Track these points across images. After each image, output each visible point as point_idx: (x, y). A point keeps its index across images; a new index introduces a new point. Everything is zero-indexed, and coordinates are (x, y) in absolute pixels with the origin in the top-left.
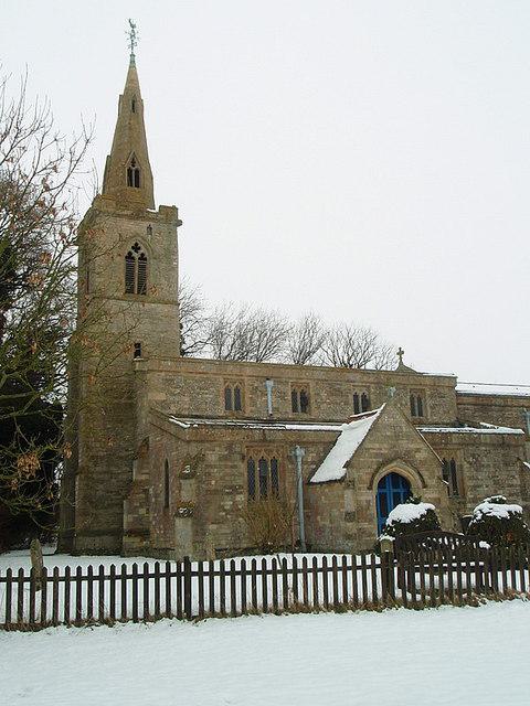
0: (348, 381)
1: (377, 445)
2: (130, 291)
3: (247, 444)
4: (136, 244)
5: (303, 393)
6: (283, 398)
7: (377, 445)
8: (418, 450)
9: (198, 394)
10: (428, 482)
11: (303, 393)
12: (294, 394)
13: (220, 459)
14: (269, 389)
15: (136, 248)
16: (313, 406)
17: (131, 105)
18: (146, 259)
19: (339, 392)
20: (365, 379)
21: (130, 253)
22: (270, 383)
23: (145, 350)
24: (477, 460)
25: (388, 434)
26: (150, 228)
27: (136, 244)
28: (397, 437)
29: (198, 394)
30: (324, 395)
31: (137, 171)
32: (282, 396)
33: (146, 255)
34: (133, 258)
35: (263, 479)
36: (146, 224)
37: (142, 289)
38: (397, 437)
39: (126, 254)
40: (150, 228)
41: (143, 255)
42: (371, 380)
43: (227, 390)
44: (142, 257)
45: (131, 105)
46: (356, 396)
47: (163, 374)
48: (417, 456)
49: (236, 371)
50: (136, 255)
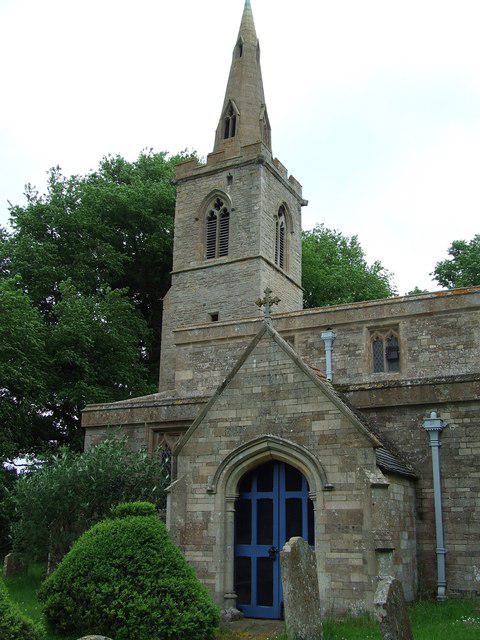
1: (232, 414)
6: (352, 354)
7: (232, 414)
8: (319, 416)
10: (336, 477)
11: (393, 339)
12: (376, 342)
14: (328, 345)
15: (218, 205)
16: (405, 358)
17: (246, 52)
19: (455, 328)
22: (326, 335)
25: (257, 390)
27: (218, 200)
28: (274, 394)
30: (424, 338)
31: (234, 120)
32: (351, 351)
36: (225, 174)
39: (208, 214)
40: (230, 178)
41: (225, 210)
45: (246, 52)
47: (191, 347)
48: (317, 427)
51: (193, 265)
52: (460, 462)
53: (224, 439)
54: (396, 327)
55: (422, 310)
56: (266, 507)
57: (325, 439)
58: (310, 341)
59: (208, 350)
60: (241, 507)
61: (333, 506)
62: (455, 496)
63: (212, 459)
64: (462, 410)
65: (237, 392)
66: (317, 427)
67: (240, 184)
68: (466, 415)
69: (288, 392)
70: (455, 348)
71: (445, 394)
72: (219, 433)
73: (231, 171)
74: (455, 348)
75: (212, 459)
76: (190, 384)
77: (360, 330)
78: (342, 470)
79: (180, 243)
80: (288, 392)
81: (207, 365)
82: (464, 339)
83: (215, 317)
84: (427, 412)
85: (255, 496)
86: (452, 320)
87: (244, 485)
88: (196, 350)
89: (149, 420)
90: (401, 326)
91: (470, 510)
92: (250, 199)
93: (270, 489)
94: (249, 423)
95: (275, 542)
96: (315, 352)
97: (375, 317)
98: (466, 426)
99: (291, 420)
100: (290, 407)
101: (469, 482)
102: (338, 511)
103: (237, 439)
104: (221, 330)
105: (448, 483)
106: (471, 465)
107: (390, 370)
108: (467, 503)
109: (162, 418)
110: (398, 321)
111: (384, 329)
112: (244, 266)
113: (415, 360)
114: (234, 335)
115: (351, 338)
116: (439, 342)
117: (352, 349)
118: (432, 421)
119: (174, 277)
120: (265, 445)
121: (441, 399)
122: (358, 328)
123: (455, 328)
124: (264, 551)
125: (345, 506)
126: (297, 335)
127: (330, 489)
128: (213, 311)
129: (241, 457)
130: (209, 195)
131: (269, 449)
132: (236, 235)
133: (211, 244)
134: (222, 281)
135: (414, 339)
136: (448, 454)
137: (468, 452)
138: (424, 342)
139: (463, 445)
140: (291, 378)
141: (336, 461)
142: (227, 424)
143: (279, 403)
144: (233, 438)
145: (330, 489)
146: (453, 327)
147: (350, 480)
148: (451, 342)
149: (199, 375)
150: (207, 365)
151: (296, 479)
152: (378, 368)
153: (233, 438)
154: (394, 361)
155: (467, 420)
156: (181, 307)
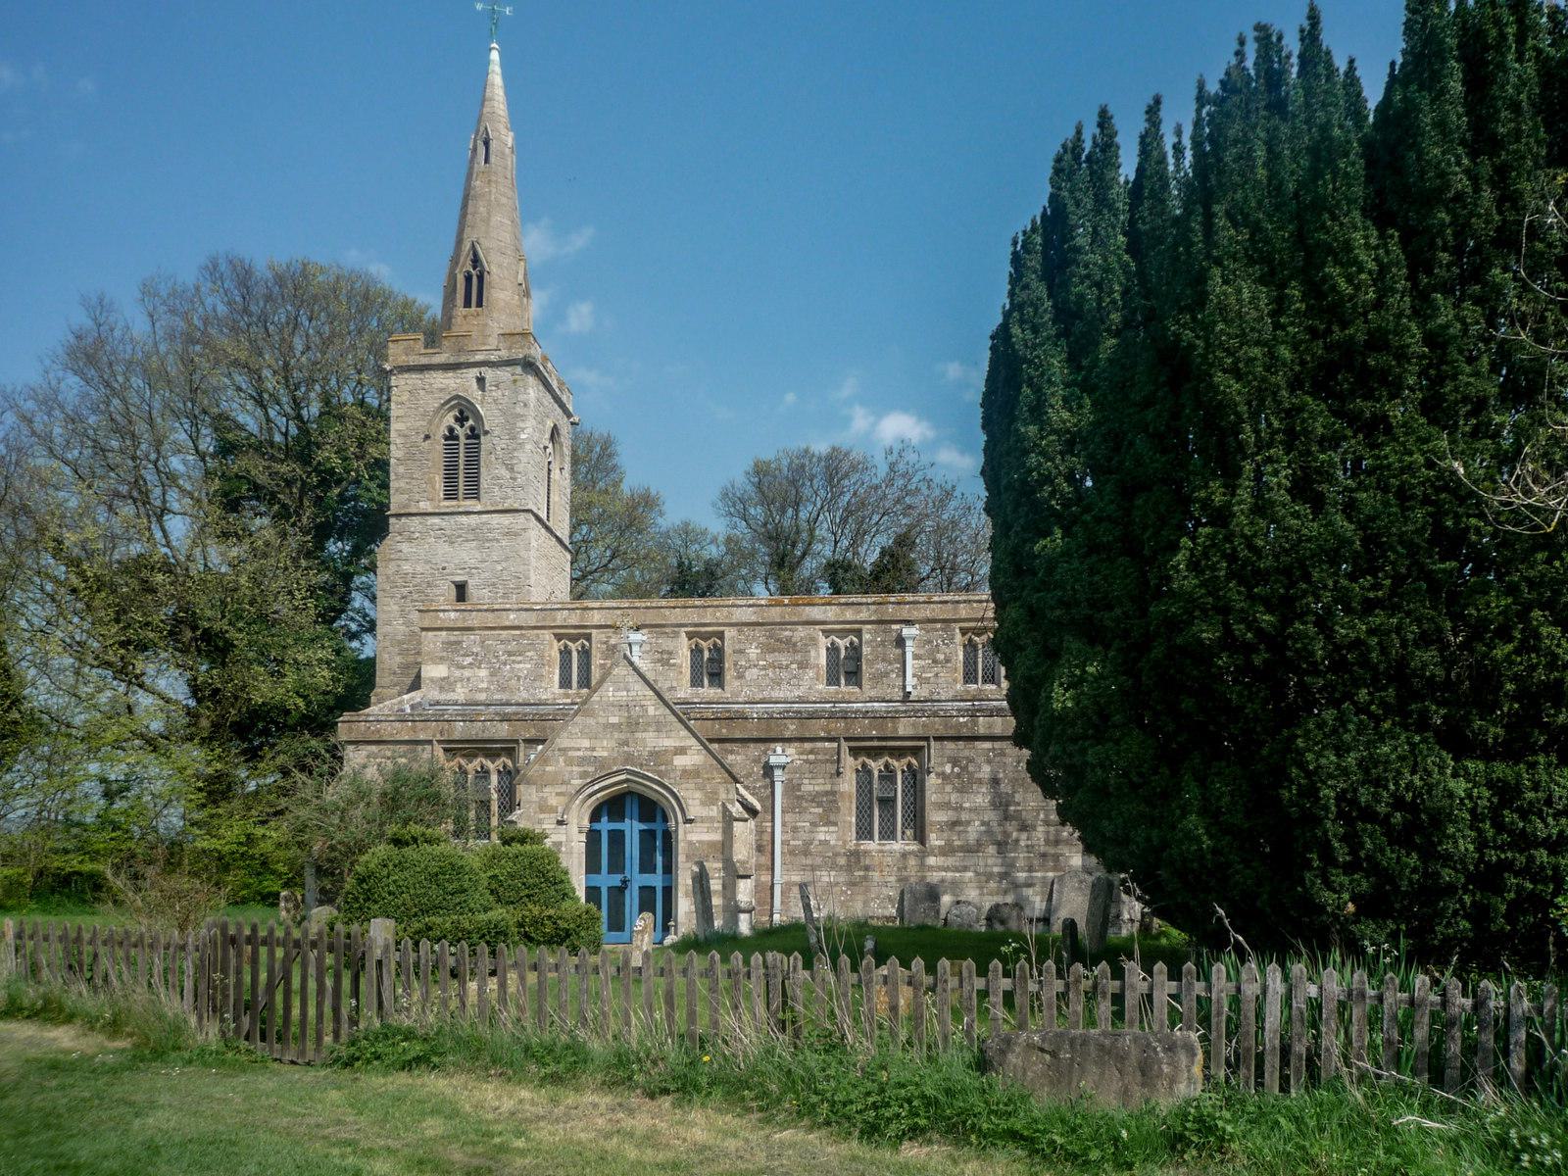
1: (586, 743)
2: (451, 494)
6: (665, 663)
7: (586, 743)
8: (682, 751)
11: (718, 652)
12: (696, 652)
16: (729, 675)
19: (790, 645)
20: (849, 615)
23: (472, 591)
24: (964, 769)
25: (614, 720)
28: (633, 725)
29: (505, 664)
30: (753, 652)
37: (474, 493)
38: (633, 725)
42: (864, 615)
43: (565, 653)
46: (833, 650)
47: (444, 633)
48: (680, 761)
51: (424, 506)
52: (801, 798)
53: (575, 768)
54: (721, 635)
55: (753, 619)
56: (617, 838)
57: (688, 774)
58: (613, 641)
59: (470, 640)
60: (593, 838)
61: (694, 837)
62: (795, 829)
63: (563, 789)
64: (808, 746)
65: (591, 721)
66: (680, 761)
67: (497, 394)
68: (811, 752)
69: (648, 724)
70: (787, 666)
71: (792, 729)
72: (570, 762)
73: (489, 374)
74: (787, 666)
75: (563, 789)
76: (445, 684)
77: (676, 635)
78: (703, 804)
79: (401, 469)
80: (648, 724)
81: (469, 660)
82: (798, 657)
83: (461, 591)
84: (772, 746)
85: (605, 826)
86: (787, 633)
87: (595, 817)
88: (452, 638)
89: (439, 737)
90: (726, 634)
91: (808, 843)
92: (512, 421)
93: (622, 819)
94: (605, 754)
95: (627, 874)
97: (696, 620)
98: (807, 761)
99: (651, 754)
100: (652, 741)
101: (808, 817)
102: (699, 842)
103: (591, 769)
104: (490, 615)
105: (789, 817)
106: (813, 801)
107: (711, 684)
108: (805, 836)
109: (456, 736)
110: (721, 629)
111: (706, 637)
112: (505, 520)
113: (741, 676)
114: (507, 624)
115: (666, 643)
116: (770, 658)
118: (780, 755)
119: (392, 520)
120: (623, 777)
121: (787, 735)
122: (674, 632)
123: (790, 645)
124: (616, 880)
125: (706, 837)
126: (594, 632)
127: (691, 821)
128: (458, 579)
129: (596, 787)
130: (443, 405)
131: (627, 781)
132: (491, 473)
133: (450, 478)
135: (741, 652)
136: (792, 788)
137: (811, 788)
138: (753, 656)
139: (806, 781)
140: (651, 711)
141: (698, 795)
142: (580, 753)
143: (639, 735)
144: (586, 768)
145: (691, 821)
146: (789, 641)
147: (711, 814)
148: (784, 659)
149: (458, 673)
150: (469, 660)
151: (650, 809)
152: (696, 682)
153: (586, 768)
154: (717, 677)
155: (812, 757)
156: (406, 567)
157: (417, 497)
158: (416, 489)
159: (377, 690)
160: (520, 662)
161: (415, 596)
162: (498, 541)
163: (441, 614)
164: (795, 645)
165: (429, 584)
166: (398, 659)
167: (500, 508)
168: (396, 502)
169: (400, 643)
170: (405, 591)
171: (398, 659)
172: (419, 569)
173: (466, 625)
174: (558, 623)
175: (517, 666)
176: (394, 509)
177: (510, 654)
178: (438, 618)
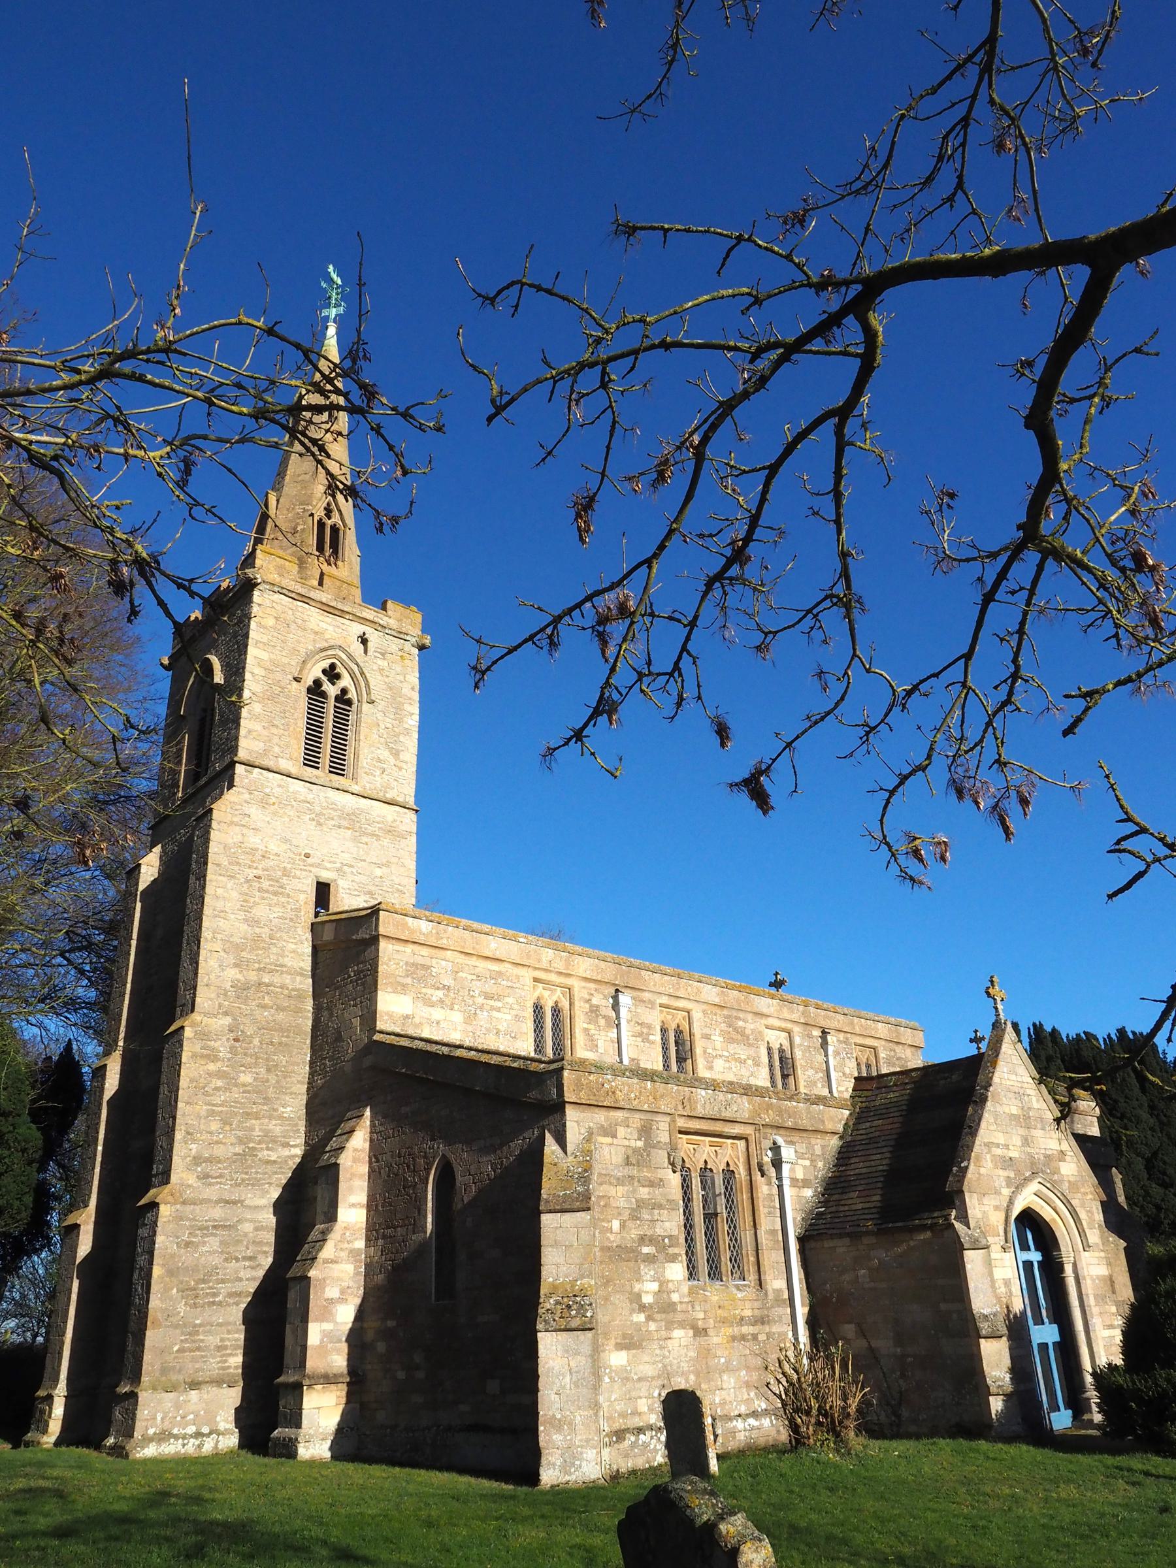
0: (758, 1014)
2: (311, 760)
3: (682, 1123)
4: (333, 666)
5: (678, 1032)
6: (646, 1040)
9: (482, 1008)
12: (664, 1031)
13: (628, 1162)
15: (332, 674)
18: (349, 703)
21: (317, 683)
26: (364, 641)
30: (718, 1039)
33: (352, 694)
34: (323, 695)
35: (710, 1217)
36: (357, 629)
39: (310, 682)
41: (344, 691)
44: (343, 698)
47: (409, 948)
49: (560, 965)
50: (332, 690)
51: (285, 765)
55: (717, 1000)
58: (595, 1001)
81: (440, 994)
86: (741, 1023)
88: (419, 960)
96: (602, 1022)
109: (700, 1111)
117: (645, 1030)
119: (239, 769)
128: (325, 876)
134: (344, 823)
138: (718, 1045)
156: (254, 840)
157: (277, 749)
158: (276, 740)
159: (196, 1017)
160: (498, 1010)
161: (266, 884)
162: (378, 838)
163: (410, 920)
164: (748, 1038)
165: (285, 872)
166: (232, 973)
167: (380, 795)
168: (247, 747)
169: (239, 948)
170: (251, 873)
171: (232, 973)
172: (273, 847)
173: (440, 943)
174: (545, 965)
175: (495, 1014)
176: (242, 754)
177: (488, 996)
178: (405, 925)
